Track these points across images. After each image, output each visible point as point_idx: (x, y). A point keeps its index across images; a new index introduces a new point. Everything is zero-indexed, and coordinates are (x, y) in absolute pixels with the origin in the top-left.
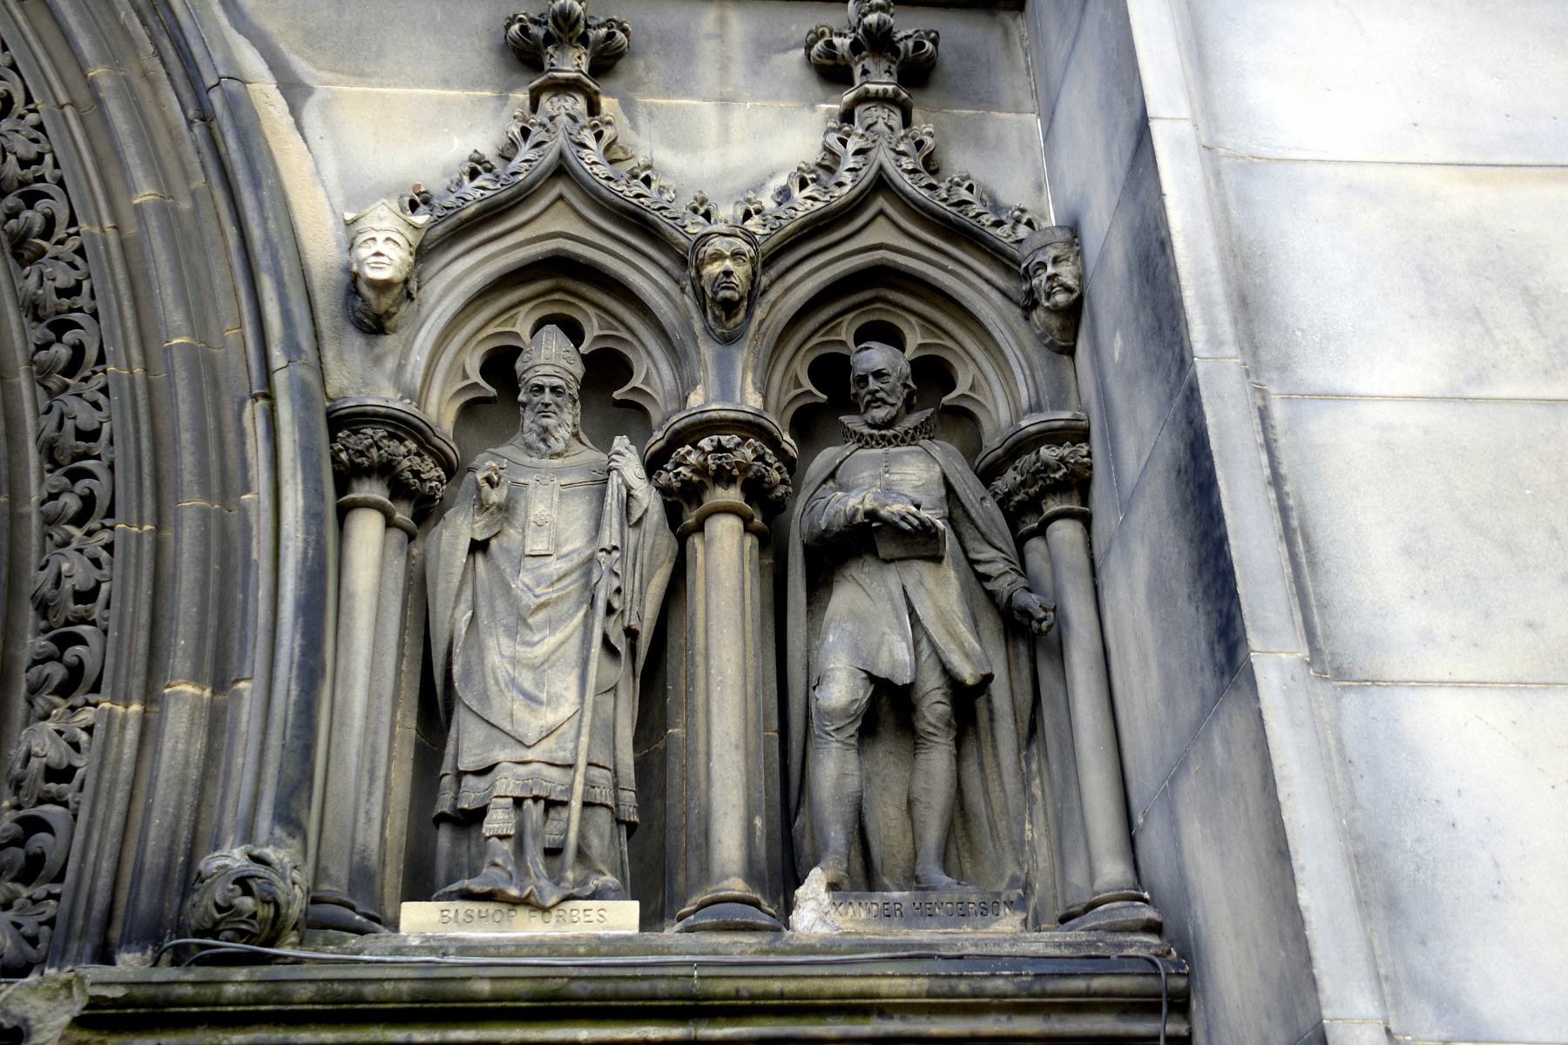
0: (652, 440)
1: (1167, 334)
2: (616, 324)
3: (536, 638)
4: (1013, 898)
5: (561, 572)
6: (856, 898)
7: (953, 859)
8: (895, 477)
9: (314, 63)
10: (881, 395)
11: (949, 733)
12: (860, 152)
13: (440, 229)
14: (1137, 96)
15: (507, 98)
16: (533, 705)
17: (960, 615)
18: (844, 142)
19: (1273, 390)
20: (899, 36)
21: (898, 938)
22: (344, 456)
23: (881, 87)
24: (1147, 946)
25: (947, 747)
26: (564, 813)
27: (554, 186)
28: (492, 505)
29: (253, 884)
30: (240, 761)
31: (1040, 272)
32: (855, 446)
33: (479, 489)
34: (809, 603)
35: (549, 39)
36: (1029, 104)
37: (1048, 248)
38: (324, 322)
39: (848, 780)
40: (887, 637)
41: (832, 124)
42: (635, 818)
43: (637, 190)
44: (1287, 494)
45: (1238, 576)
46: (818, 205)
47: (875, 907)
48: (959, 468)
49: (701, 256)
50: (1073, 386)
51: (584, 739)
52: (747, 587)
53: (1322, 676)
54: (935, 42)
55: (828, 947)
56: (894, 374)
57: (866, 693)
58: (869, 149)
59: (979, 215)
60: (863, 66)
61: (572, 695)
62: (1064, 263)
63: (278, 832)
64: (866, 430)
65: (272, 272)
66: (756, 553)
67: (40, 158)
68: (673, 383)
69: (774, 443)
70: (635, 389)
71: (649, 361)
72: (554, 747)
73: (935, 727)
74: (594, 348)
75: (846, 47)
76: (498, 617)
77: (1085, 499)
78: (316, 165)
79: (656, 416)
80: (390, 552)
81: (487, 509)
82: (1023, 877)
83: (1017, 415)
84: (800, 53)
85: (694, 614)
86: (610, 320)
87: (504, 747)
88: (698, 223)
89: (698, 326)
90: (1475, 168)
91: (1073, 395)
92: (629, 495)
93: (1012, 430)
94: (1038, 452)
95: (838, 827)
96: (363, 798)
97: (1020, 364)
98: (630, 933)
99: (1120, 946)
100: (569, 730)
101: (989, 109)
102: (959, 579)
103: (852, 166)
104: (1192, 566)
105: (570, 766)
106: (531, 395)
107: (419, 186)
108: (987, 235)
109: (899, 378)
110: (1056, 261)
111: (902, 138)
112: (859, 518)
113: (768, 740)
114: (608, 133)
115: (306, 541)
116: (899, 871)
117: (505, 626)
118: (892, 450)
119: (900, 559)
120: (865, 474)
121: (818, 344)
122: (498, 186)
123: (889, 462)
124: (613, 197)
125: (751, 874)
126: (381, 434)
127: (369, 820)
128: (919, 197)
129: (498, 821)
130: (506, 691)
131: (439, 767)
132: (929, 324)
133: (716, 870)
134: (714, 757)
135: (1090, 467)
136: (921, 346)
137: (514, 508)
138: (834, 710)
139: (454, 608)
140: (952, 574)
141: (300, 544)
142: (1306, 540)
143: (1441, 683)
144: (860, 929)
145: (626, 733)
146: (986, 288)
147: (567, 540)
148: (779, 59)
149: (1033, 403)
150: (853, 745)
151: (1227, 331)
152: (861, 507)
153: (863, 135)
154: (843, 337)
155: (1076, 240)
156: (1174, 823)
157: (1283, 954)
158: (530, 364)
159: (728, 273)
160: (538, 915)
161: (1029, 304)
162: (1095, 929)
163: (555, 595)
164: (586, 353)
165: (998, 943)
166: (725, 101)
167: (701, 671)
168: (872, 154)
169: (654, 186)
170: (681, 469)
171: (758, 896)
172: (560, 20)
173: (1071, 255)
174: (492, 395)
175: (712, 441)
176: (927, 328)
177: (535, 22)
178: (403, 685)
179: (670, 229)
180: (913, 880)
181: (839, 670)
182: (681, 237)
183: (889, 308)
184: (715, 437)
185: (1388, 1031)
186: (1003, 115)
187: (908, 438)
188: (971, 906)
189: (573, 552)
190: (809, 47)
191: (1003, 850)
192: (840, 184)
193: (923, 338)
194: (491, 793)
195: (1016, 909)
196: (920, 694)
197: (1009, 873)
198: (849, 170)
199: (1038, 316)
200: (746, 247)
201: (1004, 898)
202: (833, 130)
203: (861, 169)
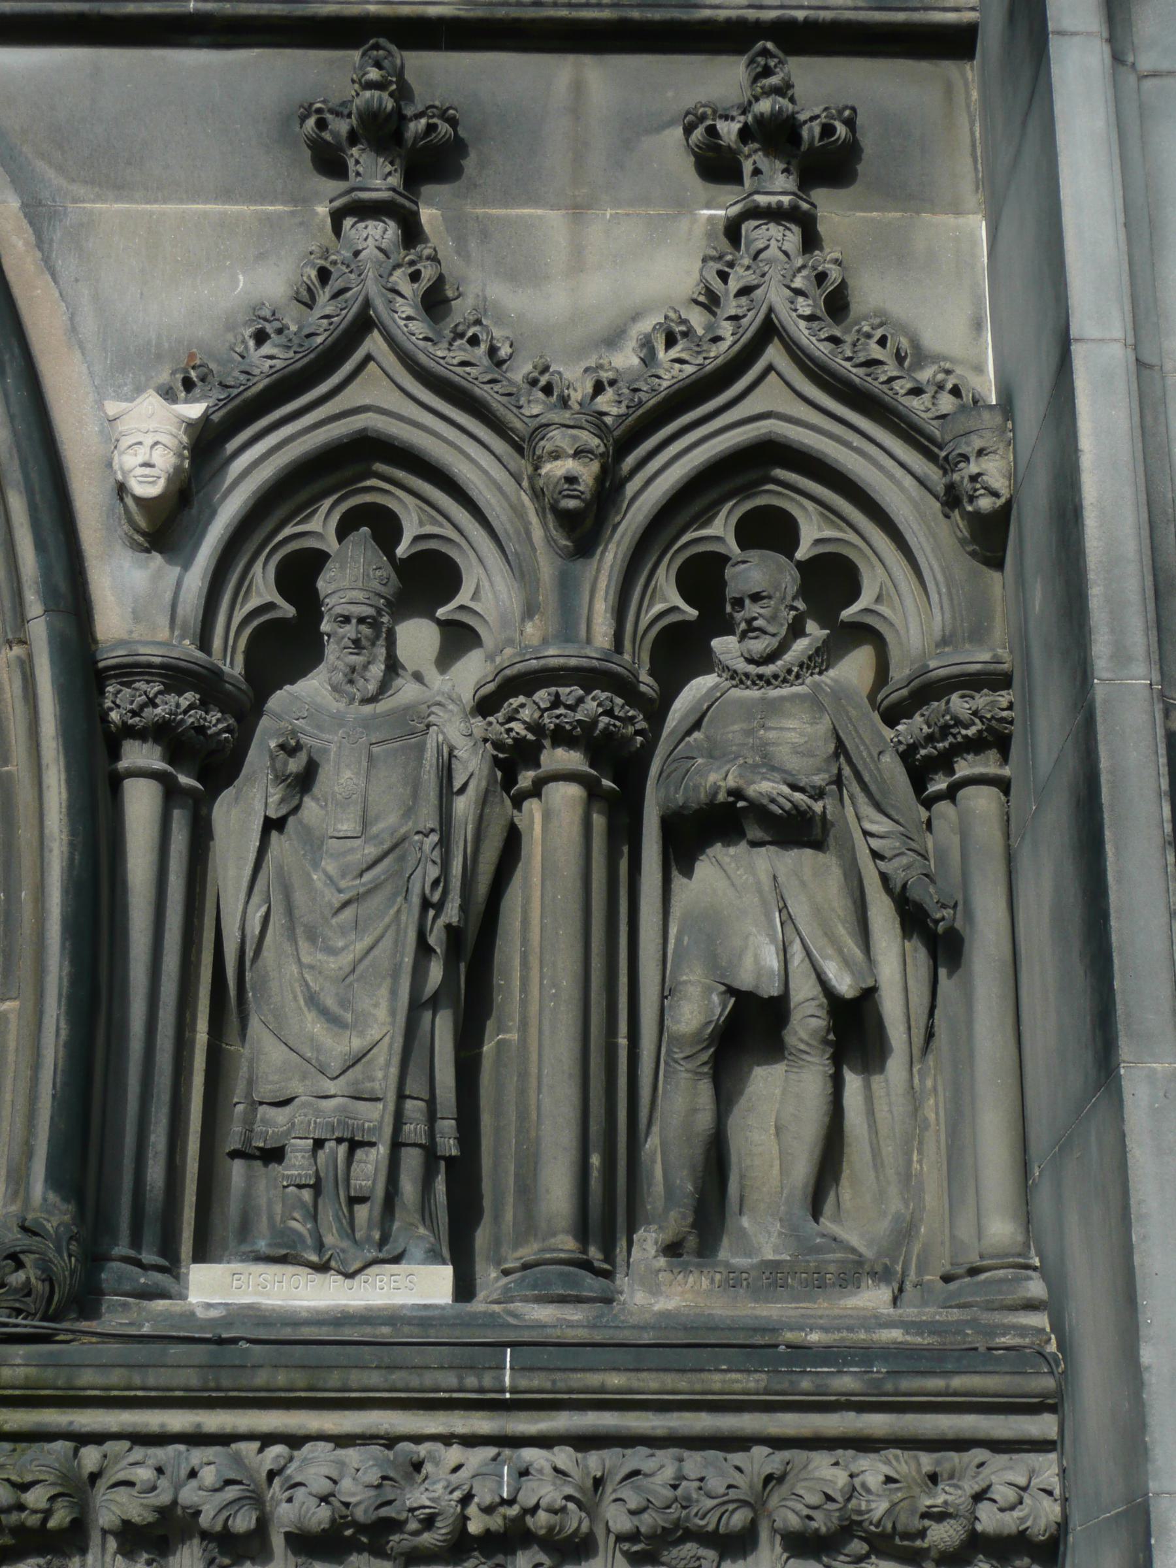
3: (340, 944)
6: (698, 1266)
8: (772, 735)
10: (759, 623)
11: (824, 1051)
17: (841, 912)
18: (724, 276)
21: (744, 1313)
23: (773, 199)
25: (821, 1068)
28: (289, 776)
31: (962, 465)
37: (973, 437)
40: (751, 938)
42: (454, 1152)
43: (461, 356)
46: (689, 369)
49: (539, 452)
54: (850, 123)
56: (778, 594)
59: (891, 380)
60: (755, 163)
61: (382, 1013)
62: (991, 456)
63: (52, 1197)
65: (22, 489)
70: (462, 608)
71: (481, 571)
73: (808, 1044)
74: (413, 550)
75: (733, 136)
76: (297, 913)
81: (284, 781)
82: (908, 1218)
84: (679, 131)
86: (434, 513)
88: (537, 401)
92: (451, 755)
94: (948, 702)
95: (685, 1173)
99: (992, 1331)
100: (380, 1056)
106: (335, 625)
108: (901, 408)
111: (799, 270)
112: (721, 797)
115: (71, 844)
117: (305, 926)
118: (773, 693)
120: (736, 727)
122: (291, 354)
126: (156, 689)
128: (818, 353)
129: (298, 1164)
130: (305, 1009)
134: (545, 1089)
135: (1011, 723)
136: (818, 542)
138: (684, 1035)
139: (247, 902)
141: (65, 849)
146: (899, 473)
148: (648, 143)
149: (947, 633)
152: (722, 784)
153: (748, 268)
155: (1010, 425)
159: (571, 480)
161: (952, 499)
164: (405, 556)
166: (578, 210)
170: (512, 725)
173: (1001, 445)
174: (290, 615)
176: (827, 517)
179: (502, 409)
182: (515, 420)
183: (779, 489)
184: (553, 689)
187: (792, 678)
190: (688, 130)
192: (716, 339)
193: (820, 529)
195: (880, 1280)
200: (594, 442)
201: (867, 1268)
202: (713, 258)
203: (745, 316)
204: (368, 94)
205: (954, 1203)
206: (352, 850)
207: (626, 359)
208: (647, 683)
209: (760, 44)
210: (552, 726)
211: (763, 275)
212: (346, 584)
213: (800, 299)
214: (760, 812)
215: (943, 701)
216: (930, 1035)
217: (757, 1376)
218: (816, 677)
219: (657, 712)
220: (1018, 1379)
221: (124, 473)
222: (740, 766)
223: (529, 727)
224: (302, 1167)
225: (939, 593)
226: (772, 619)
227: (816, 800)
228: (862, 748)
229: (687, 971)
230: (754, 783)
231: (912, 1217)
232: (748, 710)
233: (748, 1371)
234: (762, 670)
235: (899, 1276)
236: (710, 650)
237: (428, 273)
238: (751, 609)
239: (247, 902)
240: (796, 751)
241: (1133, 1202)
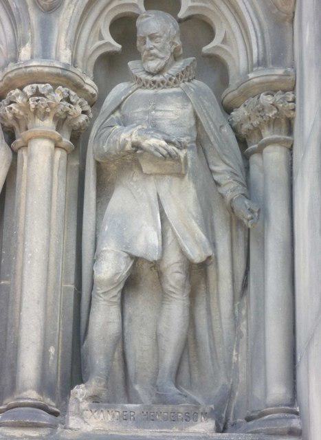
4: (207, 410)
8: (159, 114)
10: (154, 51)
11: (184, 292)
17: (194, 213)
34: (97, 203)
47: (118, 414)
48: (207, 104)
52: (55, 187)
57: (126, 267)
64: (144, 76)
68: (12, 37)
69: (78, 87)
73: (174, 288)
82: (230, 387)
95: (102, 357)
97: (255, 29)
102: (196, 188)
118: (161, 91)
120: (139, 110)
121: (117, 6)
123: (161, 99)
125: (44, 386)
133: (20, 385)
135: (294, 110)
136: (191, 8)
140: (191, 185)
144: (107, 427)
149: (260, 59)
150: (115, 302)
152: (129, 140)
170: (12, 105)
175: (32, 88)
187: (171, 83)
188: (180, 414)
191: (219, 367)
195: (209, 417)
196: (166, 265)
201: (201, 410)
208: (90, 86)
214: (152, 155)
215: (256, 98)
216: (245, 285)
218: (187, 83)
219: (95, 103)
222: (139, 130)
223: (20, 108)
225: (257, 37)
226: (162, 49)
227: (181, 149)
228: (210, 123)
229: (107, 244)
230: (146, 139)
231: (232, 387)
232: (147, 100)
234: (155, 78)
235: (224, 419)
238: (150, 44)
240: (172, 123)
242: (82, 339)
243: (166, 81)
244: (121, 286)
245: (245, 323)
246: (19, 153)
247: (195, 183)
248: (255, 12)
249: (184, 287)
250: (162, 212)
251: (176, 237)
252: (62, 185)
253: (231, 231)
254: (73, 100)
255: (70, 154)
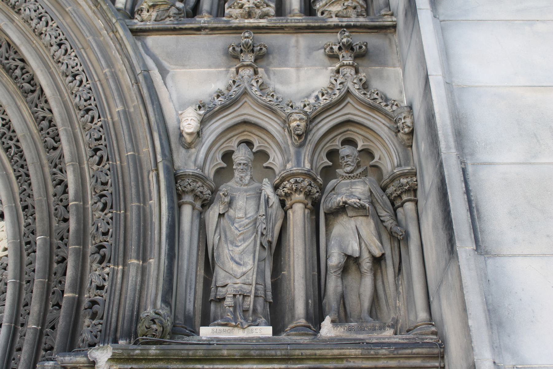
0: (276, 179)
1: (435, 144)
2: (264, 142)
3: (239, 244)
4: (390, 324)
5: (247, 223)
6: (340, 325)
7: (374, 312)
8: (353, 190)
9: (169, 63)
10: (349, 163)
12: (341, 83)
13: (208, 115)
14: (425, 67)
15: (229, 70)
16: (239, 266)
18: (336, 80)
19: (469, 162)
20: (354, 44)
22: (180, 188)
23: (348, 62)
24: (432, 339)
26: (249, 300)
27: (244, 98)
29: (156, 320)
30: (151, 284)
32: (341, 179)
33: (221, 197)
35: (241, 51)
36: (398, 64)
38: (173, 146)
39: (338, 288)
40: (351, 242)
41: (332, 75)
42: (271, 301)
43: (269, 99)
44: (472, 196)
45: (453, 223)
46: (328, 101)
48: (375, 186)
49: (290, 120)
50: (412, 158)
51: (255, 276)
52: (306, 226)
53: (481, 254)
54: (366, 46)
55: (331, 339)
58: (345, 82)
61: (251, 262)
62: (407, 118)
63: (163, 305)
64: (344, 174)
66: (309, 215)
67: (90, 98)
68: (282, 161)
69: (315, 180)
70: (270, 163)
72: (245, 278)
73: (367, 270)
76: (228, 238)
77: (415, 196)
78: (170, 96)
79: (277, 171)
80: (194, 218)
83: (394, 168)
85: (289, 235)
87: (230, 278)
88: (289, 109)
89: (290, 142)
90: (535, 87)
91: (412, 161)
92: (268, 198)
93: (391, 173)
95: (335, 303)
96: (188, 295)
98: (270, 336)
99: (423, 339)
101: (384, 66)
102: (374, 222)
103: (339, 88)
104: (443, 219)
105: (251, 284)
107: (201, 101)
109: (355, 157)
110: (404, 118)
112: (341, 204)
113: (313, 275)
114: (260, 81)
115: (169, 216)
116: (356, 316)
118: (353, 180)
119: (355, 216)
123: (353, 184)
124: (262, 101)
125: (308, 317)
127: (190, 302)
129: (229, 301)
131: (211, 285)
132: (366, 138)
133: (296, 316)
134: (296, 281)
135: (417, 185)
136: (363, 145)
137: (232, 203)
139: (214, 235)
140: (372, 221)
141: (167, 217)
142: (478, 210)
143: (519, 255)
144: (341, 334)
145: (268, 274)
146: (383, 126)
147: (249, 213)
148: (315, 53)
151: (452, 144)
154: (337, 143)
156: (439, 300)
157: (465, 340)
158: (236, 156)
159: (298, 126)
160: (241, 330)
161: (397, 131)
162: (416, 334)
163: (245, 231)
165: (384, 339)
166: (298, 68)
167: (292, 254)
168: (345, 84)
169: (275, 97)
170: (284, 189)
171: (310, 325)
172: (245, 46)
177: (237, 46)
178: (200, 259)
180: (360, 319)
181: (335, 253)
185: (494, 363)
186: (389, 68)
189: (251, 216)
192: (335, 94)
193: (363, 143)
194: (226, 293)
195: (391, 328)
197: (392, 317)
198: (338, 89)
199: (400, 135)
200: (304, 117)
201: (387, 324)
204: (245, 40)
205: (408, 311)
206: (242, 221)
207: (312, 100)
209: (342, 29)
210: (295, 188)
211: (346, 80)
212: (240, 155)
213: (356, 85)
216: (400, 269)
217: (358, 350)
219: (322, 189)
220: (431, 349)
221: (183, 127)
224: (230, 301)
233: (356, 349)
234: (350, 175)
236: (336, 172)
237: (260, 81)
239: (214, 235)
241: (463, 283)
242: (322, 298)
243: (355, 176)
244: (342, 270)
245: (401, 287)
246: (288, 211)
247: (373, 220)
248: (394, 145)
249: (371, 269)
250: (359, 234)
251: (366, 245)
252: (309, 228)
253: (391, 244)
254: (312, 185)
255: (312, 212)
